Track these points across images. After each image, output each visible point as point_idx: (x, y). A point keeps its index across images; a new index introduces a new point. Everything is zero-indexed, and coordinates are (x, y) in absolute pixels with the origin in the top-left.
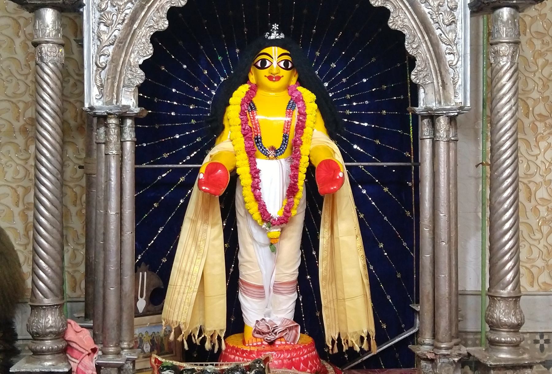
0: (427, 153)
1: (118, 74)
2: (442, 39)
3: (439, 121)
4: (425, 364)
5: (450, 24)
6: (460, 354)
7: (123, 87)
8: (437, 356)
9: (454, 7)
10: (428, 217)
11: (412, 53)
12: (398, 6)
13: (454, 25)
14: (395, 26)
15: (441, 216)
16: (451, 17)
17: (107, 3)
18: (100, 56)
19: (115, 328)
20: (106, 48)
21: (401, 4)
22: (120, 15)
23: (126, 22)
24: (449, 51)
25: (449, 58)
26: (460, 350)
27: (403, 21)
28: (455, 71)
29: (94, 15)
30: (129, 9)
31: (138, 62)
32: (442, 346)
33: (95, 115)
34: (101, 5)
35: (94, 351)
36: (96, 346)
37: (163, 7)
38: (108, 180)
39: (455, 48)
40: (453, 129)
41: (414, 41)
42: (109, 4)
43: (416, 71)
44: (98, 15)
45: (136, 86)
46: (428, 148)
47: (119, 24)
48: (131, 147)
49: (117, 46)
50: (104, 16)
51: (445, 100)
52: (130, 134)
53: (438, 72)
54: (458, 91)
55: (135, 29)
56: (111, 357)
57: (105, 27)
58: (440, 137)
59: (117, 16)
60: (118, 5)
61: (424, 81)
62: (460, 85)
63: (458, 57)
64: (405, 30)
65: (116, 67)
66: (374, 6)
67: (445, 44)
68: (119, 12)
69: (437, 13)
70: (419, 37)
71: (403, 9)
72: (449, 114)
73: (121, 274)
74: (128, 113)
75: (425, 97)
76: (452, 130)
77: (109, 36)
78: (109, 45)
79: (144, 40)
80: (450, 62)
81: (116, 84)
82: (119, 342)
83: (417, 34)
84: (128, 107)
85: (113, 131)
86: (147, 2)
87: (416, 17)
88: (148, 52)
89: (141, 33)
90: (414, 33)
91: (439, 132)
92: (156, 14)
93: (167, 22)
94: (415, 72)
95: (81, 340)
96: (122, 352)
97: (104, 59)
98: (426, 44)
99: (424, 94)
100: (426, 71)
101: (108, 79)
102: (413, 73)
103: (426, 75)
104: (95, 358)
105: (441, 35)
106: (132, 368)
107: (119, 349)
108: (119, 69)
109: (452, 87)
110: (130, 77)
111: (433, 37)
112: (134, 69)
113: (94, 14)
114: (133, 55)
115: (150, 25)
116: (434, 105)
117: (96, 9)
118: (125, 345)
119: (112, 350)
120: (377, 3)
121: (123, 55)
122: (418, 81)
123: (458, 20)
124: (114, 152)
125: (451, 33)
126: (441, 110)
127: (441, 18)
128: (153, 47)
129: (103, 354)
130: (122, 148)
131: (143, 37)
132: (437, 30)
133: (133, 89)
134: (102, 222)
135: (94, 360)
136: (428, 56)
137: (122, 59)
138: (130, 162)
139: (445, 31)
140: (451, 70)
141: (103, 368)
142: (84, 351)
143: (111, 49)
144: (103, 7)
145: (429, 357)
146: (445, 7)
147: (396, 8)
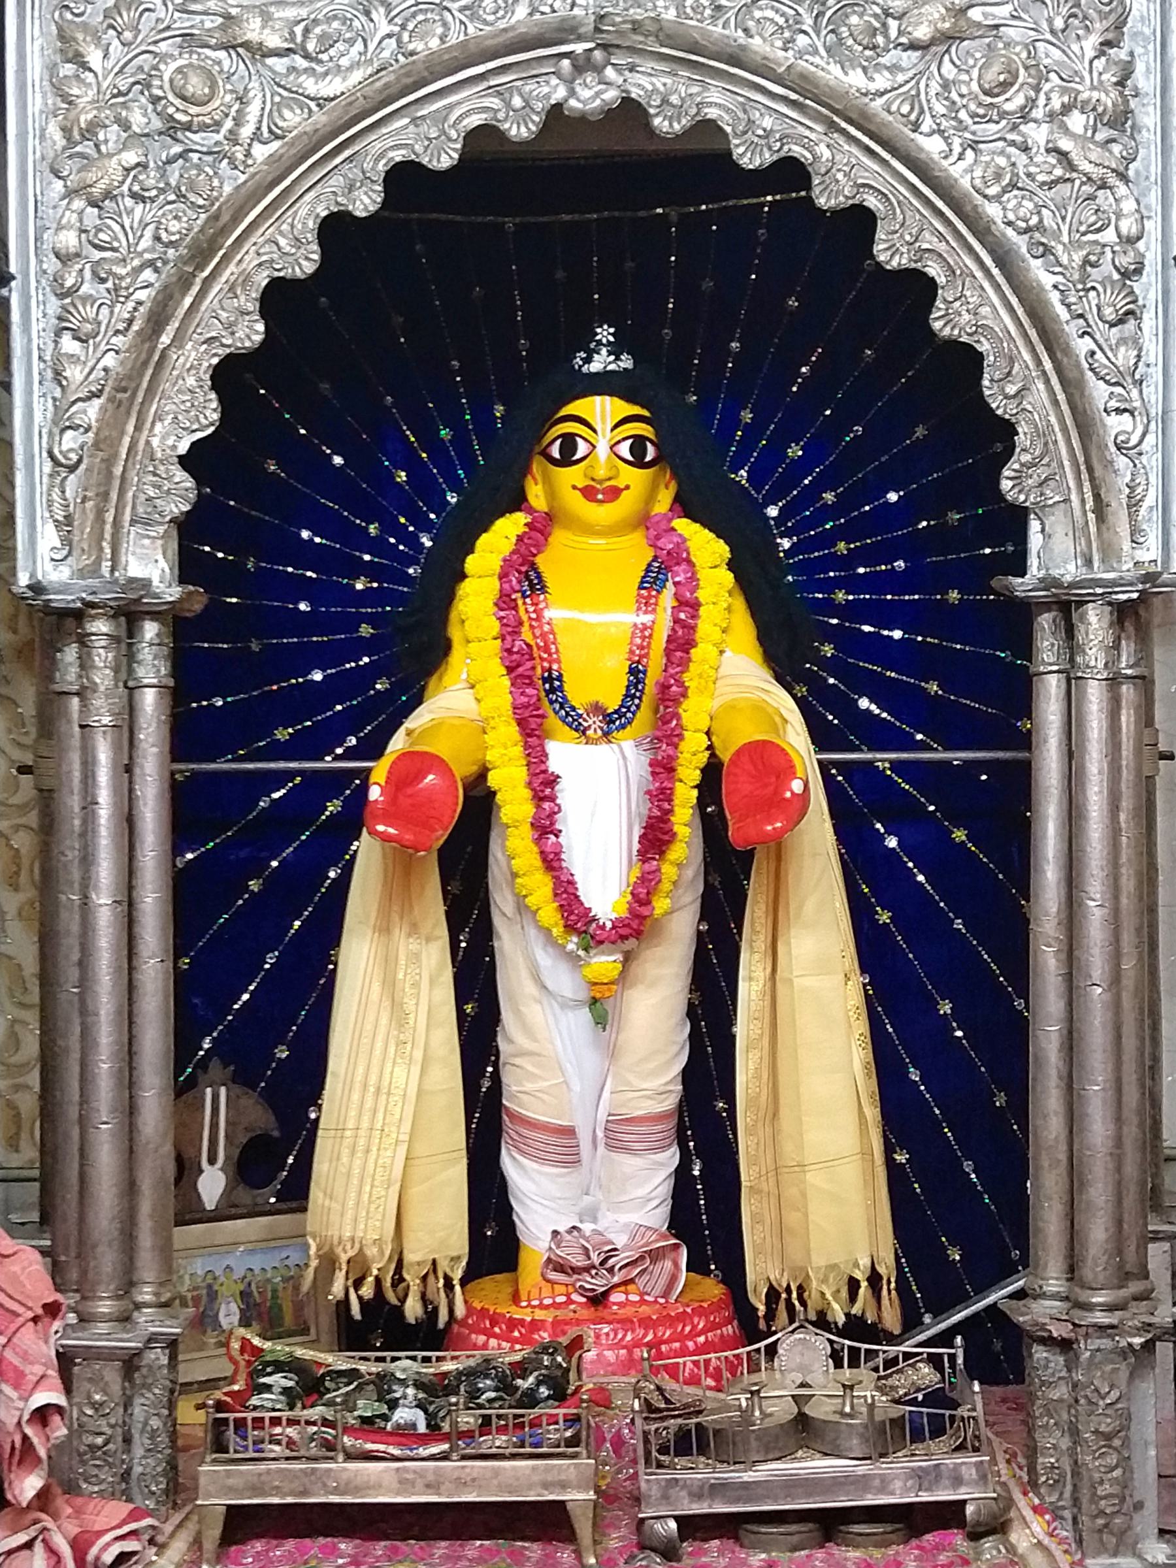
0: (1052, 717)
1: (116, 483)
2: (1096, 365)
3: (1083, 618)
4: (1045, 1355)
5: (1121, 321)
6: (1150, 1325)
7: (133, 522)
8: (1077, 1329)
9: (1133, 267)
10: (1054, 910)
11: (1005, 412)
12: (960, 268)
13: (1132, 321)
14: (952, 329)
15: (1088, 906)
16: (1124, 297)
17: (81, 270)
18: (63, 431)
19: (116, 1242)
20: (80, 404)
21: (969, 262)
22: (119, 305)
23: (135, 327)
24: (1118, 405)
25: (1116, 424)
26: (1152, 1314)
27: (976, 314)
28: (1135, 466)
29: (42, 307)
30: (146, 287)
31: (174, 447)
32: (1094, 1300)
33: (48, 610)
34: (62, 277)
35: (52, 1310)
36: (59, 1297)
37: (247, 279)
38: (89, 804)
39: (1135, 393)
40: (1133, 645)
41: (1009, 374)
42: (88, 274)
43: (1016, 466)
44: (54, 306)
45: (171, 521)
46: (1053, 700)
47: (117, 332)
48: (157, 704)
49: (111, 400)
50: (72, 310)
51: (1103, 551)
52: (154, 666)
53: (1083, 468)
54: (1144, 527)
55: (165, 349)
56: (103, 1328)
57: (77, 343)
58: (1088, 667)
59: (111, 307)
60: (115, 275)
61: (1041, 495)
62: (1151, 508)
63: (1145, 421)
64: (982, 339)
65: (109, 462)
66: (888, 267)
67: (1107, 382)
68: (118, 296)
69: (1080, 286)
70: (1025, 361)
71: (974, 277)
72: (1114, 597)
73: (131, 1085)
74: (145, 601)
75: (1044, 547)
76: (1128, 646)
77: (87, 370)
78: (88, 399)
79: (191, 381)
80: (1120, 438)
81: (109, 517)
82: (128, 1285)
83: (1019, 352)
84: (146, 584)
85: (103, 656)
86: (200, 267)
87: (1014, 301)
88: (206, 418)
89: (181, 360)
90: (1010, 350)
91: (1084, 651)
92: (226, 302)
93: (260, 327)
94: (1014, 470)
95: (14, 1278)
96: (136, 1314)
97: (74, 439)
98: (1047, 381)
99: (1040, 536)
100: (1048, 465)
101: (83, 502)
102: (1006, 473)
103: (1047, 479)
104: (57, 1332)
105: (1093, 353)
106: (165, 1361)
107: (125, 1304)
108: (118, 470)
109: (1124, 514)
110: (152, 494)
111: (1065, 360)
112: (162, 468)
113: (44, 304)
114: (158, 427)
115: (209, 335)
116: (1070, 571)
117: (48, 289)
118: (146, 1294)
119: (105, 1307)
120: (897, 257)
121: (130, 428)
122: (1022, 498)
123: (1144, 306)
124: (106, 720)
125: (1122, 349)
126: (1086, 584)
127: (1094, 302)
128: (221, 400)
129: (81, 1321)
130: (131, 709)
131: (189, 370)
132: (1079, 341)
133: (161, 529)
134: (75, 928)
135: (52, 1340)
136: (1053, 419)
137: (127, 440)
138: (155, 750)
139: (1106, 340)
140: (1122, 462)
141: (78, 1361)
142: (20, 1309)
143: (92, 411)
144: (69, 282)
145: (1055, 1335)
146: (1107, 268)
147: (954, 272)
